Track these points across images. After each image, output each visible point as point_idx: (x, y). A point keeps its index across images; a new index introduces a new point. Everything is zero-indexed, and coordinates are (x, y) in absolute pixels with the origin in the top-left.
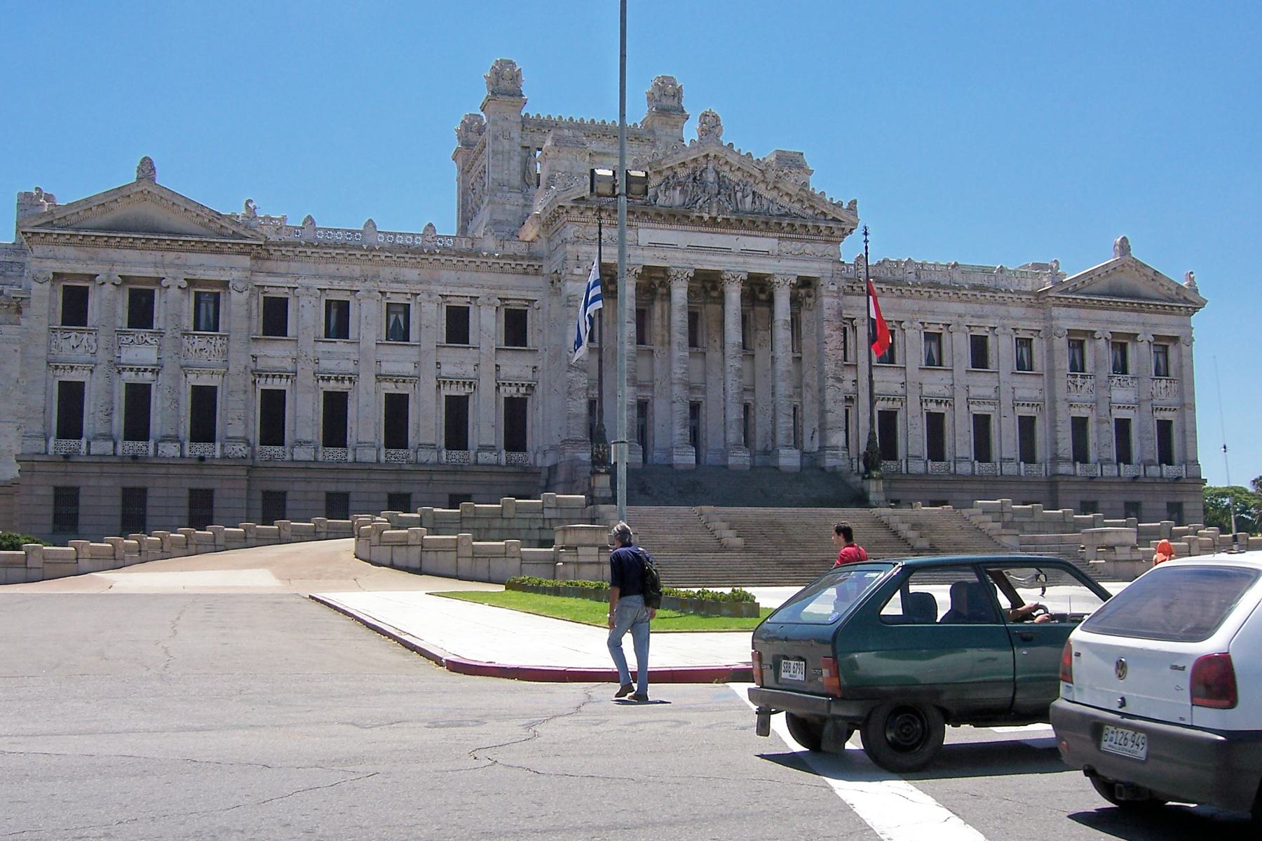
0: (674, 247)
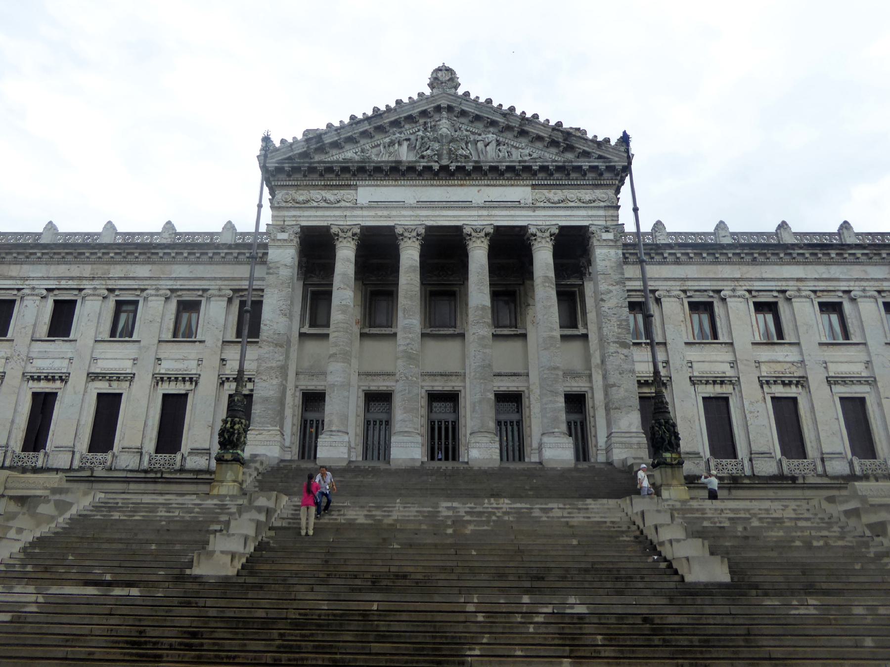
0: (401, 205)
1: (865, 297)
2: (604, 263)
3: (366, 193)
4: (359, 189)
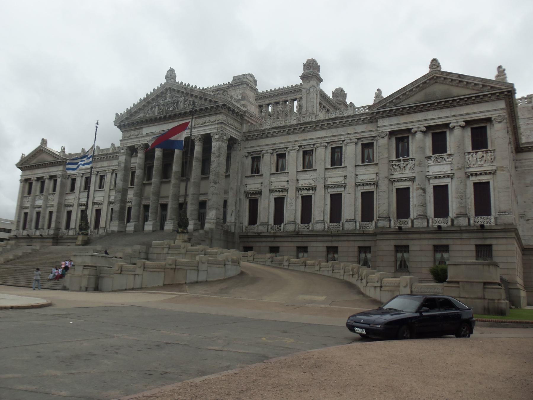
1: (351, 143)
2: (215, 149)
3: (146, 130)
4: (144, 129)
